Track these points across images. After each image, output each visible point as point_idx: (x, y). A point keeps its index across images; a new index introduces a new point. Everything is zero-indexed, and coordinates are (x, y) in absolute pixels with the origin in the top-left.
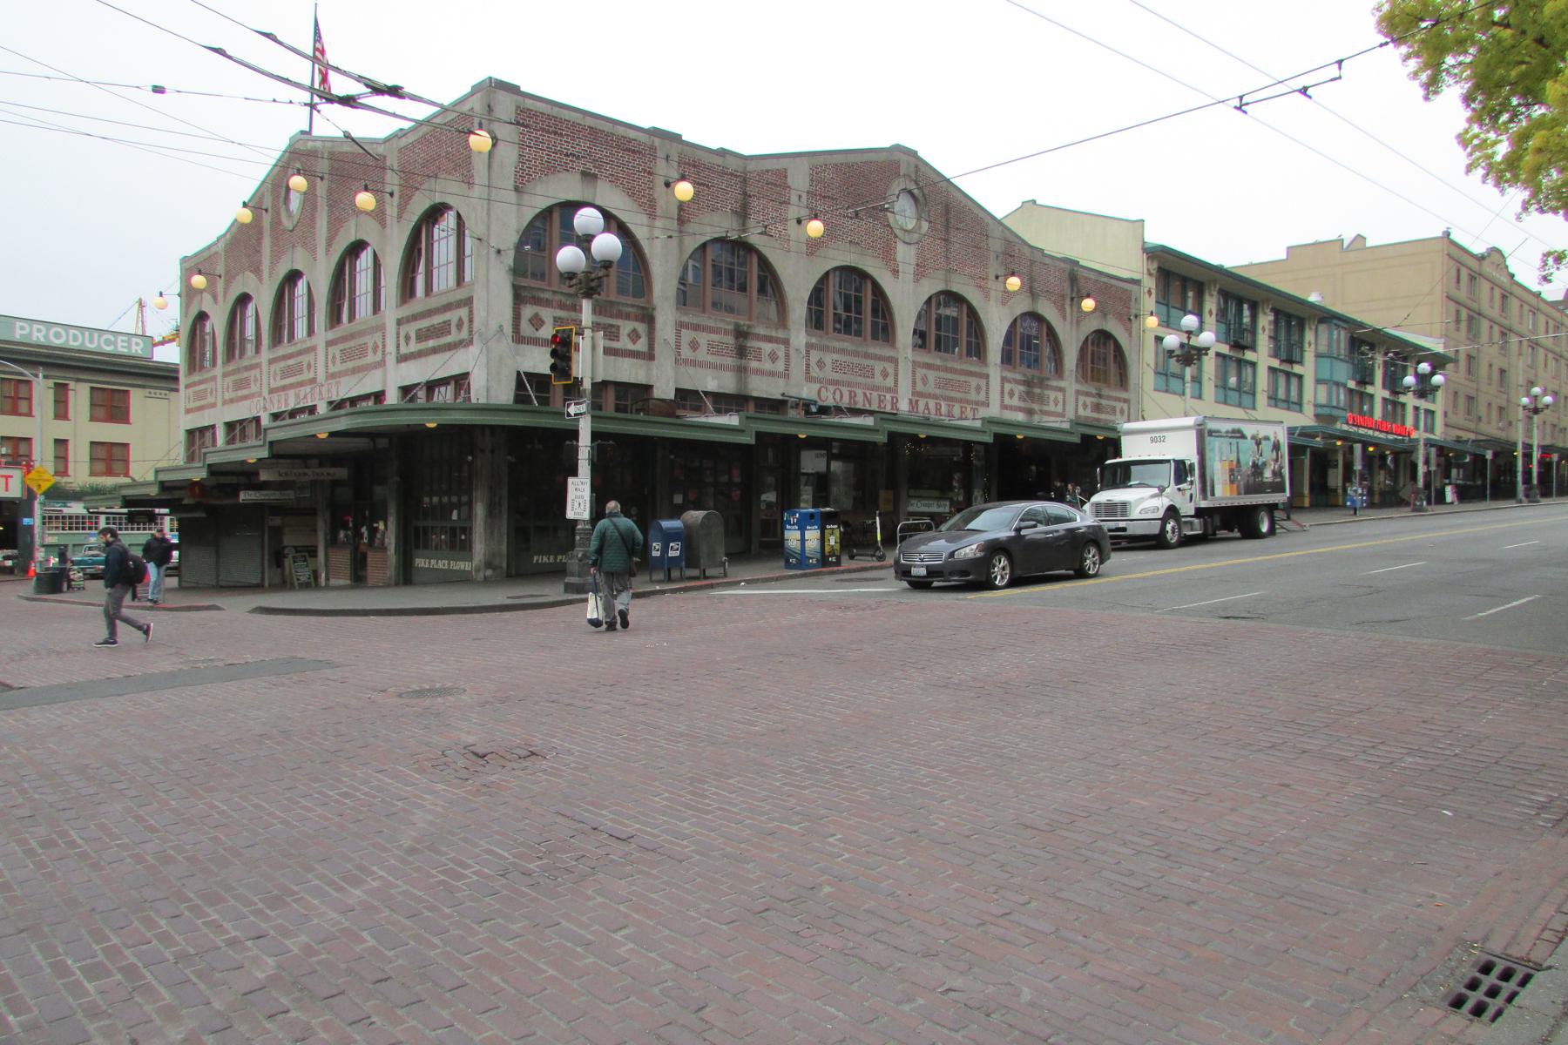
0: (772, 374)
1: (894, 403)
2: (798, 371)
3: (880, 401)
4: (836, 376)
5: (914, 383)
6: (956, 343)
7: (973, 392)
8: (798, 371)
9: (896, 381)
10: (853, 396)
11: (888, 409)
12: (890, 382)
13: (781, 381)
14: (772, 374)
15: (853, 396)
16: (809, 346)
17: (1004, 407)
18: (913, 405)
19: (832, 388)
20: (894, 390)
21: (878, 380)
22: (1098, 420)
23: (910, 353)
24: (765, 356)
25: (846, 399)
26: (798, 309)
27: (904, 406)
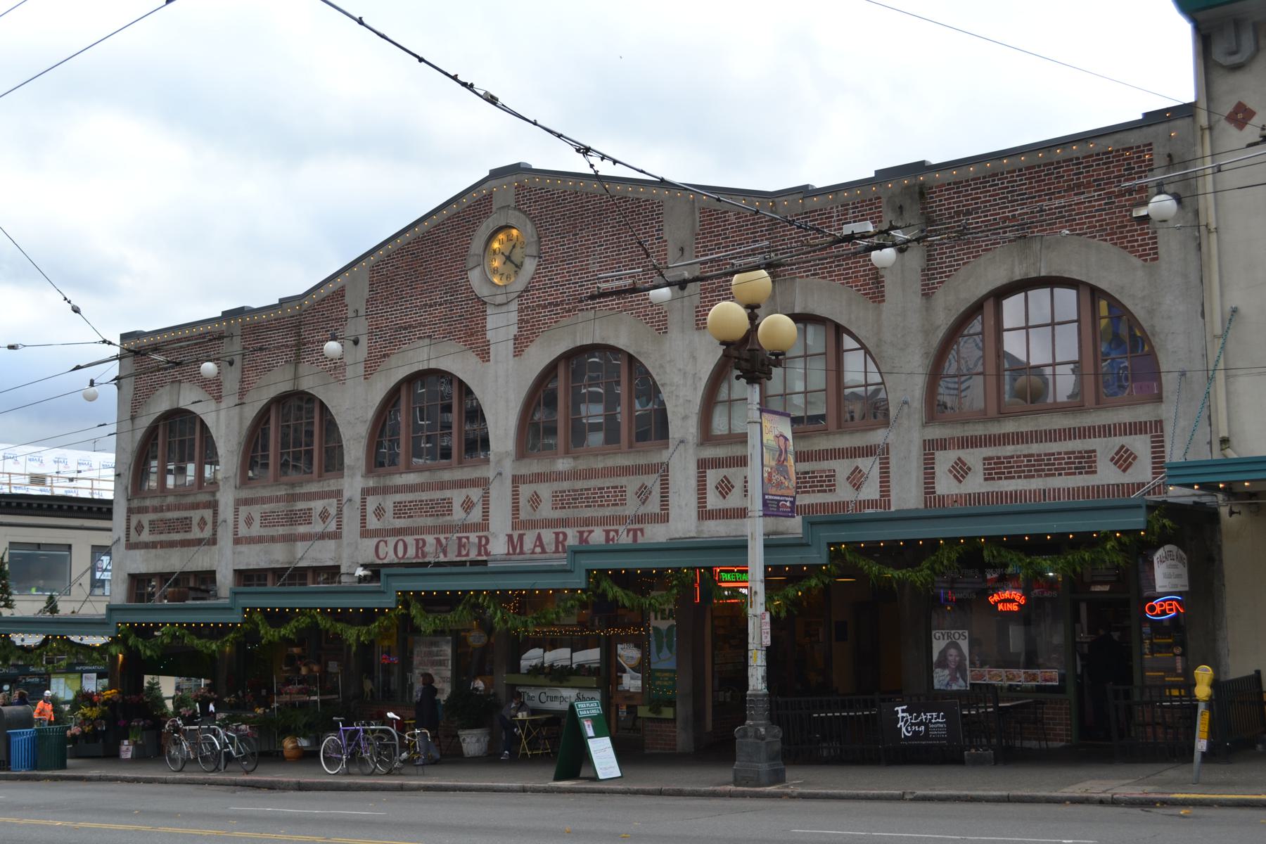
0: (323, 536)
1: (482, 546)
2: (351, 526)
3: (461, 546)
4: (400, 523)
5: (516, 509)
6: (552, 430)
7: (195, 529)
8: (351, 526)
9: (486, 513)
10: (421, 545)
11: (473, 555)
12: (476, 515)
13: (331, 544)
14: (323, 536)
15: (421, 545)
16: (366, 492)
17: (705, 514)
18: (515, 544)
19: (392, 541)
20: (484, 526)
21: (458, 515)
22: (1000, 496)
23: (509, 468)
24: (457, 507)
25: (411, 552)
26: (355, 450)
27: (498, 547)
